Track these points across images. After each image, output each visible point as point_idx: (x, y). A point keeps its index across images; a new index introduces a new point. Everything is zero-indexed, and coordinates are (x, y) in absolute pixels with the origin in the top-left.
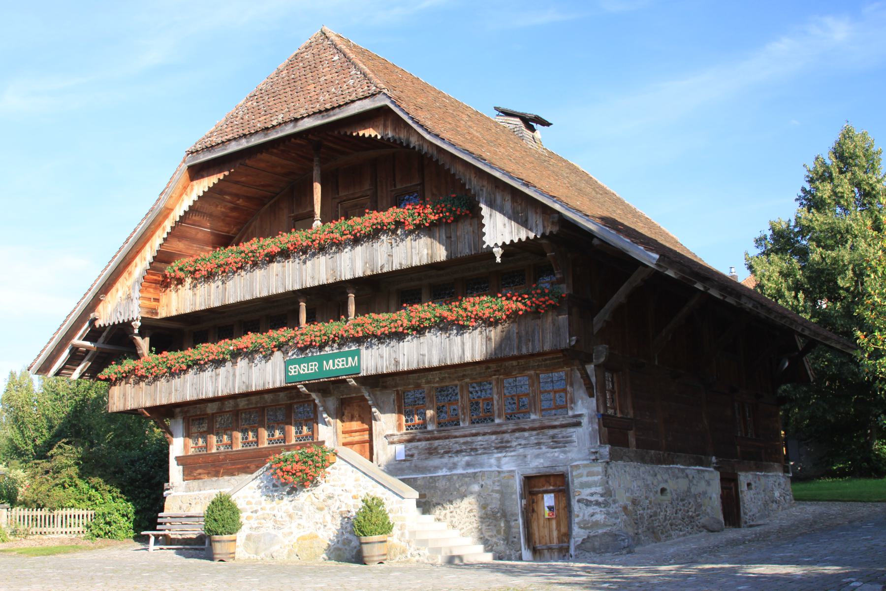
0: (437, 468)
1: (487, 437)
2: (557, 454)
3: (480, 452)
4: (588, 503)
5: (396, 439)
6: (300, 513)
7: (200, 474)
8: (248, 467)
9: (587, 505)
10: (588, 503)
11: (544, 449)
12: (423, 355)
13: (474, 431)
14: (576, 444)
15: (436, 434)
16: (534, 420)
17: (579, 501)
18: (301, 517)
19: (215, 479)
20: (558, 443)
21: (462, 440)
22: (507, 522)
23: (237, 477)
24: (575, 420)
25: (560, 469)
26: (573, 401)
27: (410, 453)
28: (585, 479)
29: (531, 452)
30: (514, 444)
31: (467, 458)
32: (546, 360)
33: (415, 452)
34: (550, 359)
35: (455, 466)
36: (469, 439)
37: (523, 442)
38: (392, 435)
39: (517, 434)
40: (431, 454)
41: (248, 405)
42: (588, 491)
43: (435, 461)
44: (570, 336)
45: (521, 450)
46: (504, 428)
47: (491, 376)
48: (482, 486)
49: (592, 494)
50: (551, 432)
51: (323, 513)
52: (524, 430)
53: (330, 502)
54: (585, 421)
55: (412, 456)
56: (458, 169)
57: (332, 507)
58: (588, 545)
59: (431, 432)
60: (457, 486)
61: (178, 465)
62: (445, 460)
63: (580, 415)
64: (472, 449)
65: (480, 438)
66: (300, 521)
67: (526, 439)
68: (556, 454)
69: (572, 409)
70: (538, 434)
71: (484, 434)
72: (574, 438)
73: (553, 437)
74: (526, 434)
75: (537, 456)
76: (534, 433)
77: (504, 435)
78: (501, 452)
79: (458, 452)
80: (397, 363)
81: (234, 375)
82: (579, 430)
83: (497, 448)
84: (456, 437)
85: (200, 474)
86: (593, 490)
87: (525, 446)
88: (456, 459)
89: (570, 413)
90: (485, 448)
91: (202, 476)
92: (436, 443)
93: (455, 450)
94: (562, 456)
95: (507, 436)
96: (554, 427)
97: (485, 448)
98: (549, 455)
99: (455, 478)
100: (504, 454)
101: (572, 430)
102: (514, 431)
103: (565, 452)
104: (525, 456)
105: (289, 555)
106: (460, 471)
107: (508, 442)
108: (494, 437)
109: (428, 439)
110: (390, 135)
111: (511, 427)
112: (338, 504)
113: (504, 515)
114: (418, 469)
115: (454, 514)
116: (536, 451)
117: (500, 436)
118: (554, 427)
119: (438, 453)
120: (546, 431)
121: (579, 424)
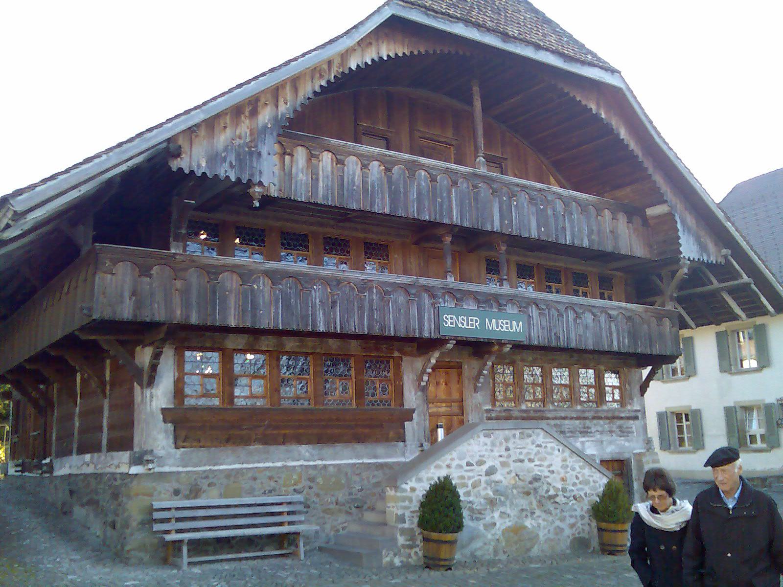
1: (573, 422)
2: (622, 441)
3: (568, 435)
5: (493, 415)
6: (503, 499)
12: (580, 335)
13: (563, 415)
18: (503, 504)
20: (624, 432)
25: (626, 456)
26: (632, 399)
29: (606, 438)
36: (558, 422)
37: (600, 429)
39: (595, 421)
41: (300, 347)
45: (599, 436)
52: (600, 418)
53: (536, 485)
57: (540, 491)
61: (165, 421)
65: (567, 422)
66: (502, 509)
70: (609, 423)
71: (572, 418)
72: (634, 429)
73: (620, 427)
74: (601, 422)
75: (610, 443)
76: (607, 421)
80: (558, 338)
81: (361, 308)
82: (637, 422)
83: (581, 433)
84: (548, 418)
87: (602, 432)
90: (571, 432)
94: (627, 444)
95: (587, 422)
96: (621, 418)
98: (618, 442)
100: (587, 439)
101: (631, 422)
102: (594, 418)
103: (629, 441)
104: (602, 442)
105: (496, 552)
108: (577, 422)
112: (545, 487)
116: (609, 438)
118: (621, 418)
120: (615, 421)
121: (636, 418)
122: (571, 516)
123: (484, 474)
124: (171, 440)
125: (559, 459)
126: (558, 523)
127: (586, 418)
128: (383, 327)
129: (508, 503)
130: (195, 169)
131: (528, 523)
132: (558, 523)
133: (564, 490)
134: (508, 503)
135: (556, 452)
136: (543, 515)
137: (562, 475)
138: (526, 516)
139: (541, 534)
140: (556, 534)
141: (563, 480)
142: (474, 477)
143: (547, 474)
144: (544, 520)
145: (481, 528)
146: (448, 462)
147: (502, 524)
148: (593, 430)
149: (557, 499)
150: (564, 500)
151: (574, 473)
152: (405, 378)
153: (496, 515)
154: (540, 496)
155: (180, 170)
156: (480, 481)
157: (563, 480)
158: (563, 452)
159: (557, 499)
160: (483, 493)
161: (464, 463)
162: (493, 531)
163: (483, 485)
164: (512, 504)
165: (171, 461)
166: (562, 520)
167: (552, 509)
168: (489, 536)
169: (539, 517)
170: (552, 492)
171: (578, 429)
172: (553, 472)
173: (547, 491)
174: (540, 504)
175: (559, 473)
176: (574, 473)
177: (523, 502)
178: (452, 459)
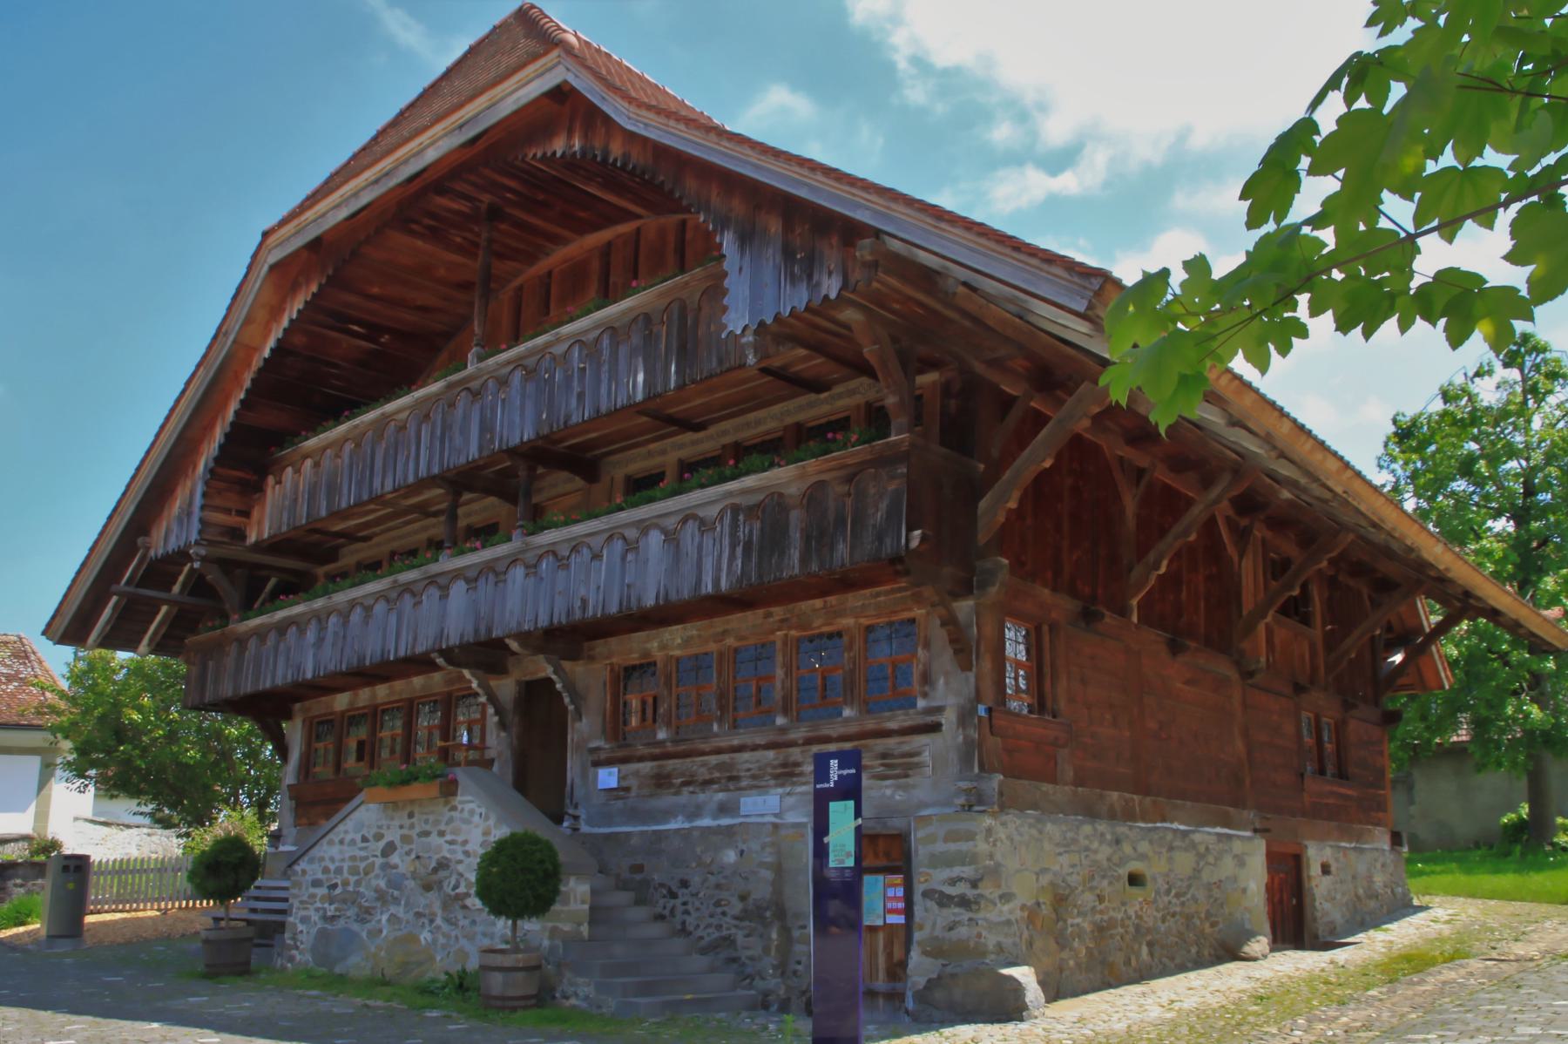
0: (668, 814)
1: (759, 754)
3: (744, 783)
4: (944, 901)
5: (603, 756)
6: (396, 893)
9: (941, 905)
10: (944, 901)
13: (736, 742)
14: (929, 771)
15: (670, 748)
16: (848, 720)
17: (926, 894)
18: (396, 901)
21: (713, 760)
22: (785, 931)
24: (929, 719)
25: (897, 824)
27: (624, 784)
28: (940, 847)
31: (721, 796)
32: (878, 595)
33: (633, 782)
34: (887, 593)
35: (696, 812)
36: (725, 757)
38: (597, 749)
40: (659, 786)
42: (946, 873)
43: (667, 800)
44: (910, 529)
46: (793, 736)
47: (773, 632)
48: (742, 852)
49: (953, 882)
51: (429, 895)
53: (442, 874)
54: (948, 719)
55: (627, 789)
57: (445, 884)
59: (662, 742)
60: (698, 850)
62: (685, 797)
63: (939, 710)
64: (731, 778)
65: (746, 756)
66: (393, 909)
68: (888, 792)
69: (925, 695)
71: (755, 748)
73: (884, 756)
77: (791, 750)
78: (782, 785)
79: (707, 783)
83: (776, 777)
84: (703, 753)
86: (957, 871)
88: (701, 797)
90: (754, 777)
92: (671, 764)
93: (701, 779)
97: (754, 777)
99: (696, 834)
100: (788, 789)
103: (905, 788)
106: (706, 822)
107: (797, 764)
108: (771, 754)
109: (654, 758)
113: (781, 913)
114: (635, 815)
115: (689, 907)
119: (671, 785)
121: (935, 728)
122: (485, 935)
125: (479, 831)
126: (463, 942)
127: (792, 744)
135: (476, 818)
136: (445, 927)
142: (366, 858)
143: (460, 856)
144: (444, 935)
145: (364, 935)
149: (468, 902)
153: (384, 918)
158: (487, 818)
159: (468, 902)
160: (374, 883)
161: (358, 837)
163: (377, 871)
164: (407, 904)
166: (471, 938)
167: (460, 916)
171: (769, 770)
173: (456, 887)
174: (445, 907)
178: (346, 832)
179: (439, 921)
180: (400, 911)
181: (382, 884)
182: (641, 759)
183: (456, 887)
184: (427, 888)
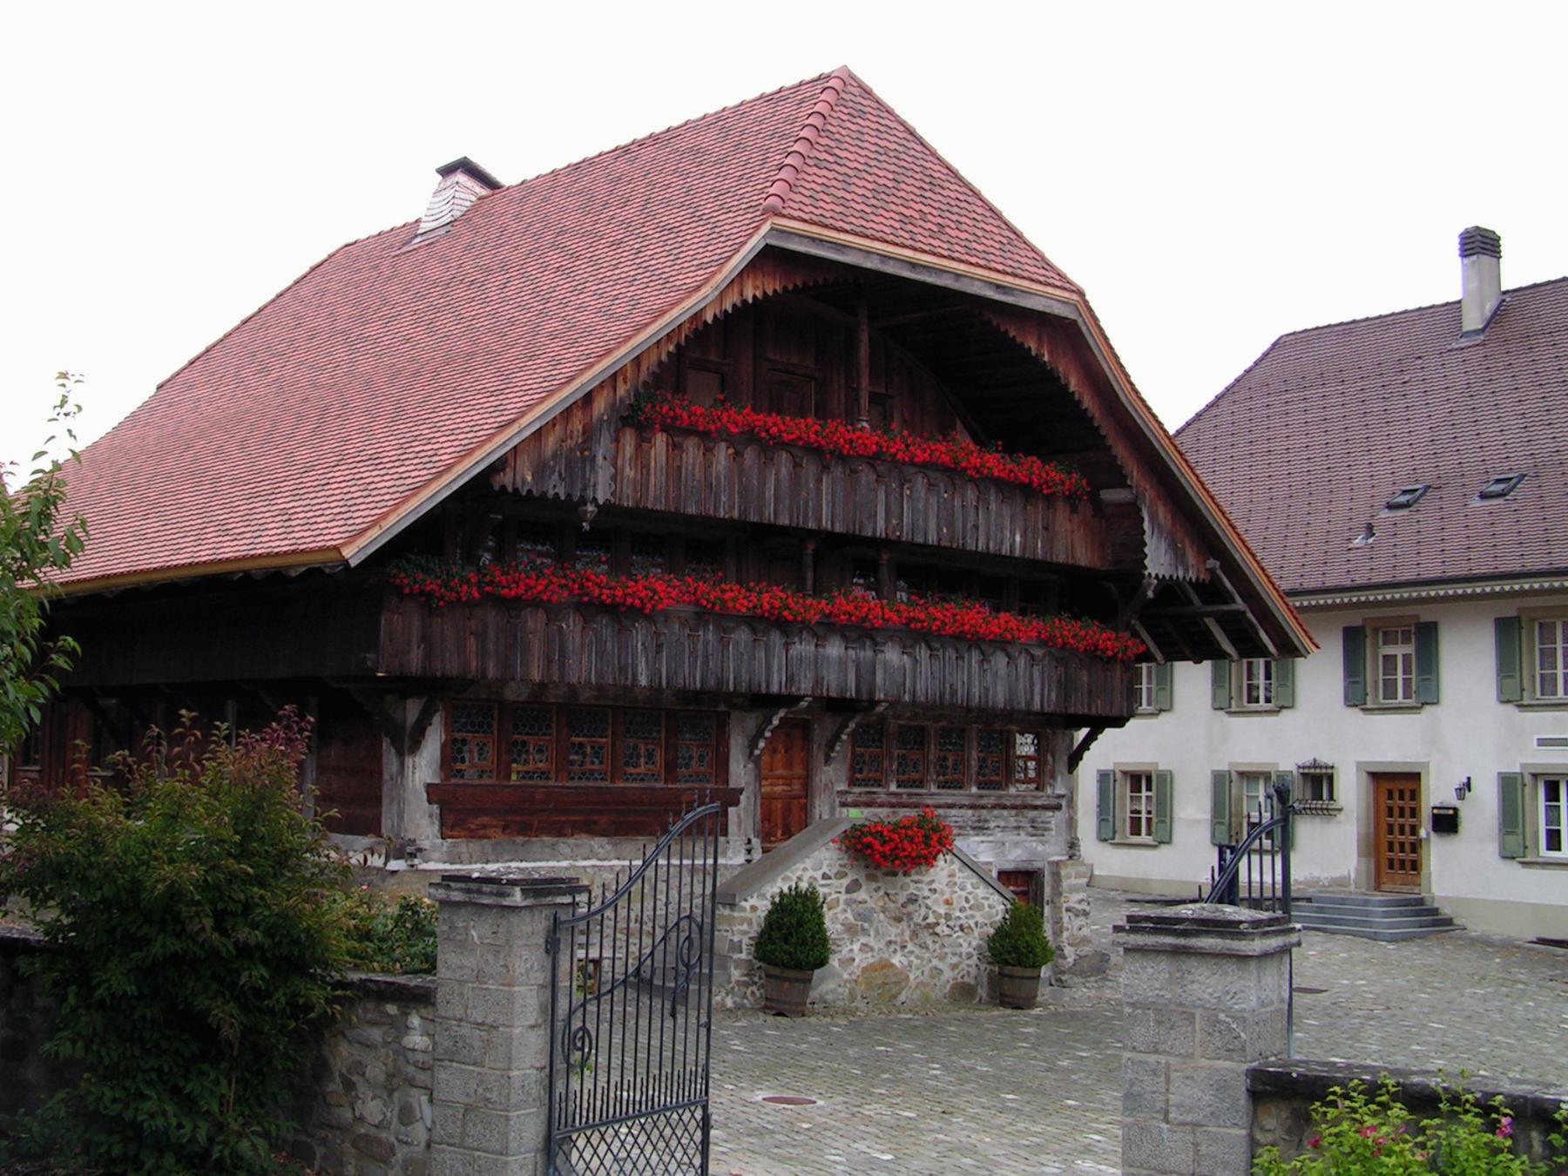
1: (962, 811)
2: (1034, 844)
5: (850, 799)
6: (866, 925)
7: (484, 827)
8: (595, 822)
11: (1023, 836)
12: (987, 689)
18: (865, 931)
19: (520, 839)
20: (1038, 830)
23: (571, 841)
25: (1037, 865)
26: (1053, 776)
29: (1010, 837)
30: (992, 825)
37: (1002, 824)
39: (996, 812)
46: (984, 801)
50: (1031, 814)
52: (1005, 807)
53: (911, 908)
56: (1121, 452)
58: (1078, 967)
65: (954, 812)
66: (863, 940)
67: (1005, 819)
71: (961, 807)
73: (1033, 821)
74: (1005, 813)
75: (1016, 844)
76: (1013, 812)
80: (954, 693)
81: (693, 654)
82: (1057, 813)
85: (484, 827)
89: (1049, 791)
91: (490, 832)
94: (1040, 848)
95: (984, 812)
96: (1036, 808)
101: (1050, 813)
102: (994, 807)
103: (1043, 843)
105: (852, 998)
107: (986, 821)
108: (970, 812)
109: (892, 805)
110: (1046, 358)
111: (992, 801)
112: (923, 911)
117: (977, 813)
118: (1036, 808)
121: (1058, 808)
122: (954, 954)
123: (843, 890)
124: (437, 827)
125: (945, 873)
126: (935, 962)
127: (983, 807)
128: (721, 680)
129: (872, 932)
130: (519, 485)
131: (896, 960)
132: (935, 962)
133: (948, 916)
134: (872, 932)
136: (917, 950)
137: (947, 896)
138: (895, 951)
139: (912, 977)
140: (933, 977)
141: (947, 902)
143: (927, 893)
146: (799, 873)
147: (861, 960)
148: (992, 825)
149: (938, 930)
150: (947, 931)
151: (964, 894)
152: (733, 743)
153: (856, 947)
154: (917, 924)
155: (503, 488)
156: (838, 900)
157: (947, 902)
158: (952, 863)
159: (938, 930)
160: (841, 917)
162: (850, 969)
163: (842, 906)
164: (877, 932)
165: (436, 855)
166: (942, 958)
167: (929, 942)
168: (846, 976)
169: (912, 952)
170: (931, 920)
172: (935, 891)
173: (925, 918)
175: (942, 893)
176: (964, 894)
177: (893, 932)
178: (805, 869)
179: (910, 947)
180: (872, 941)
181: (849, 915)
182: (881, 805)
183: (925, 918)
184: (899, 920)
